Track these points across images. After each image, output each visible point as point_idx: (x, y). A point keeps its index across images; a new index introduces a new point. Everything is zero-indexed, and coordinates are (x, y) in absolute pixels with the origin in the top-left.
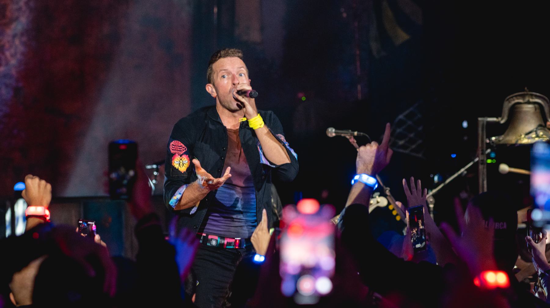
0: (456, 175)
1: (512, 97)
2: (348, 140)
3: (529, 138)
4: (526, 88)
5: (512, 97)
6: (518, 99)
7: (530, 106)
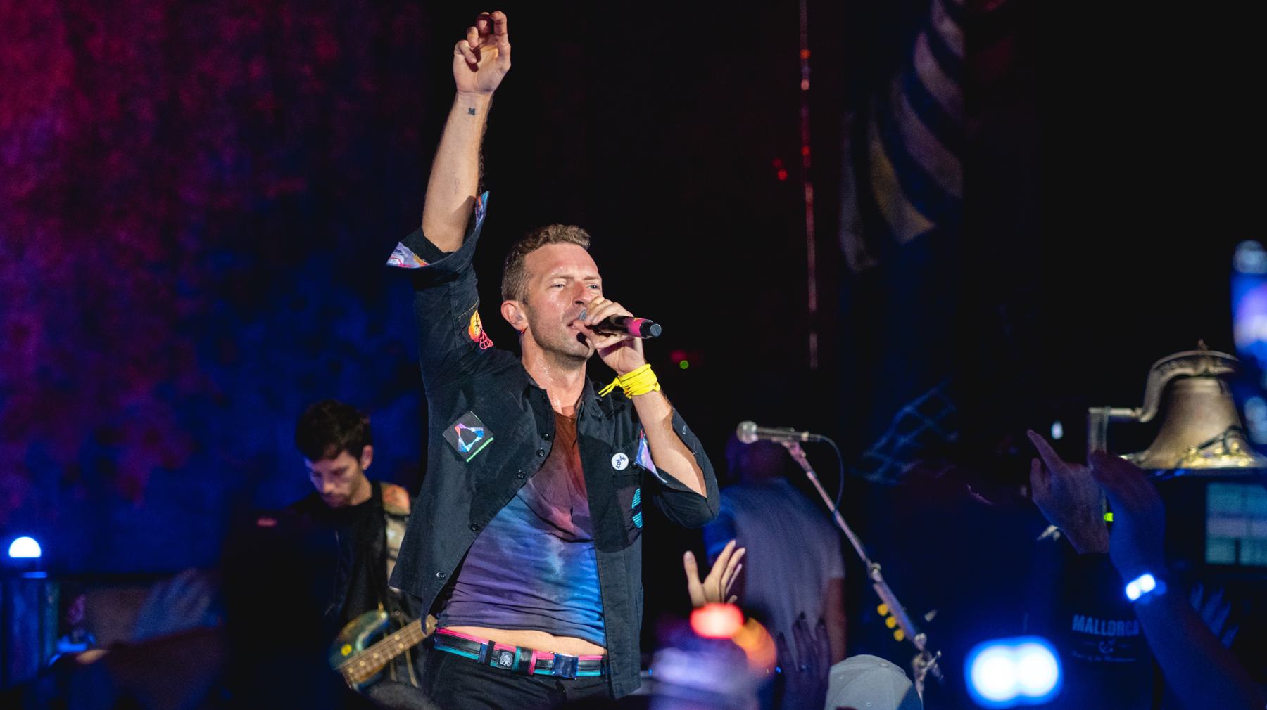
1: (1168, 362)
2: (786, 451)
3: (1206, 457)
4: (1201, 342)
5: (1168, 362)
6: (1182, 367)
7: (1210, 383)
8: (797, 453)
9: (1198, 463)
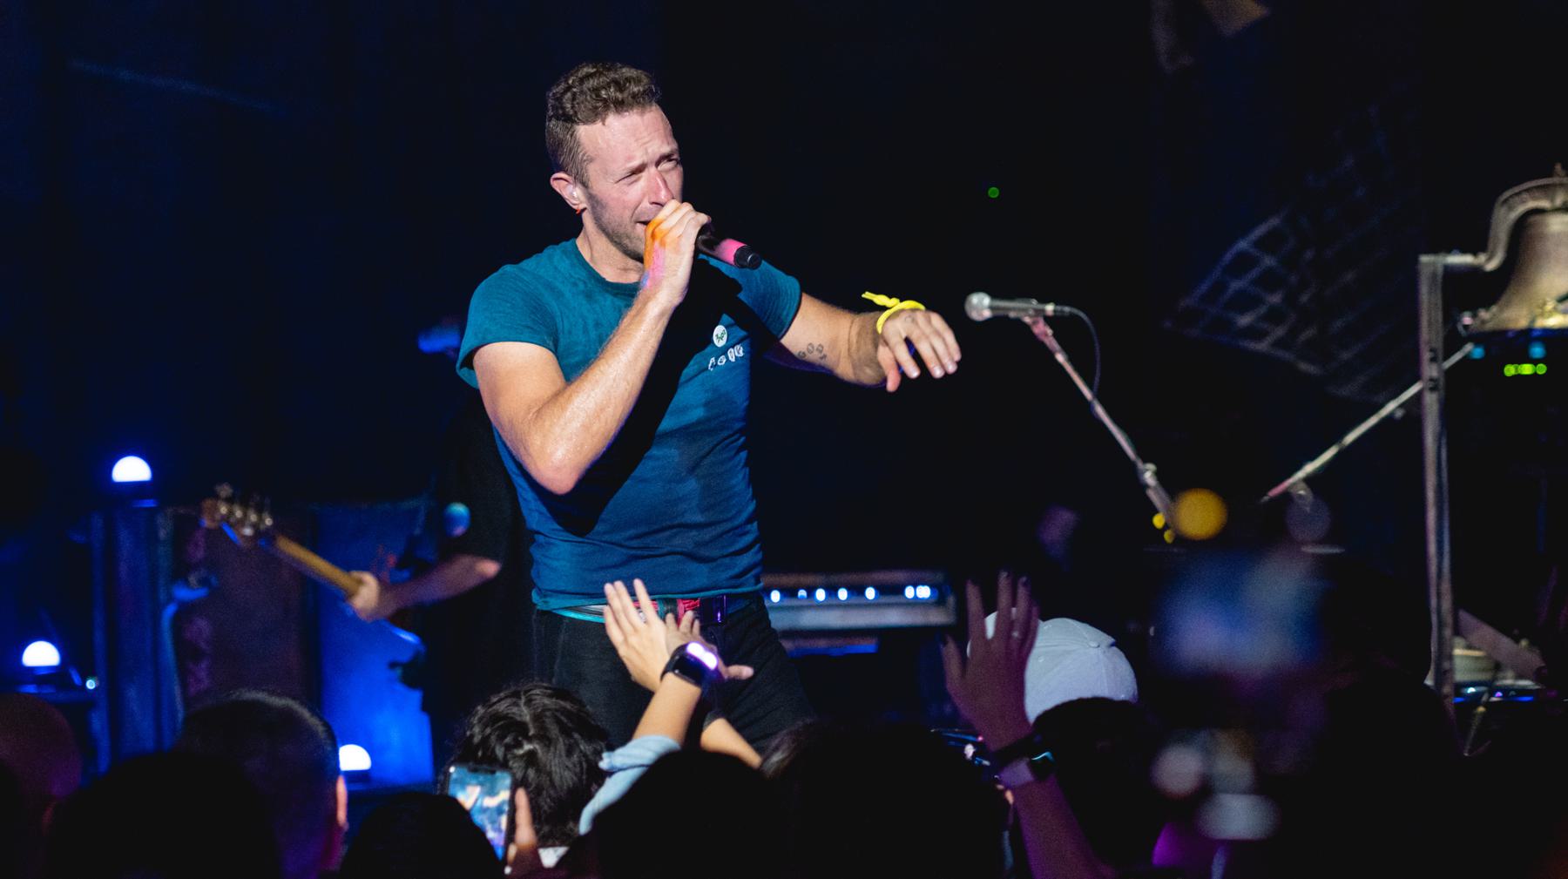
0: (1373, 421)
2: (1027, 327)
4: (1558, 167)
6: (1535, 199)
8: (1043, 330)
9: (1555, 321)
